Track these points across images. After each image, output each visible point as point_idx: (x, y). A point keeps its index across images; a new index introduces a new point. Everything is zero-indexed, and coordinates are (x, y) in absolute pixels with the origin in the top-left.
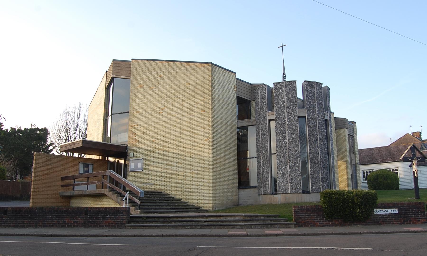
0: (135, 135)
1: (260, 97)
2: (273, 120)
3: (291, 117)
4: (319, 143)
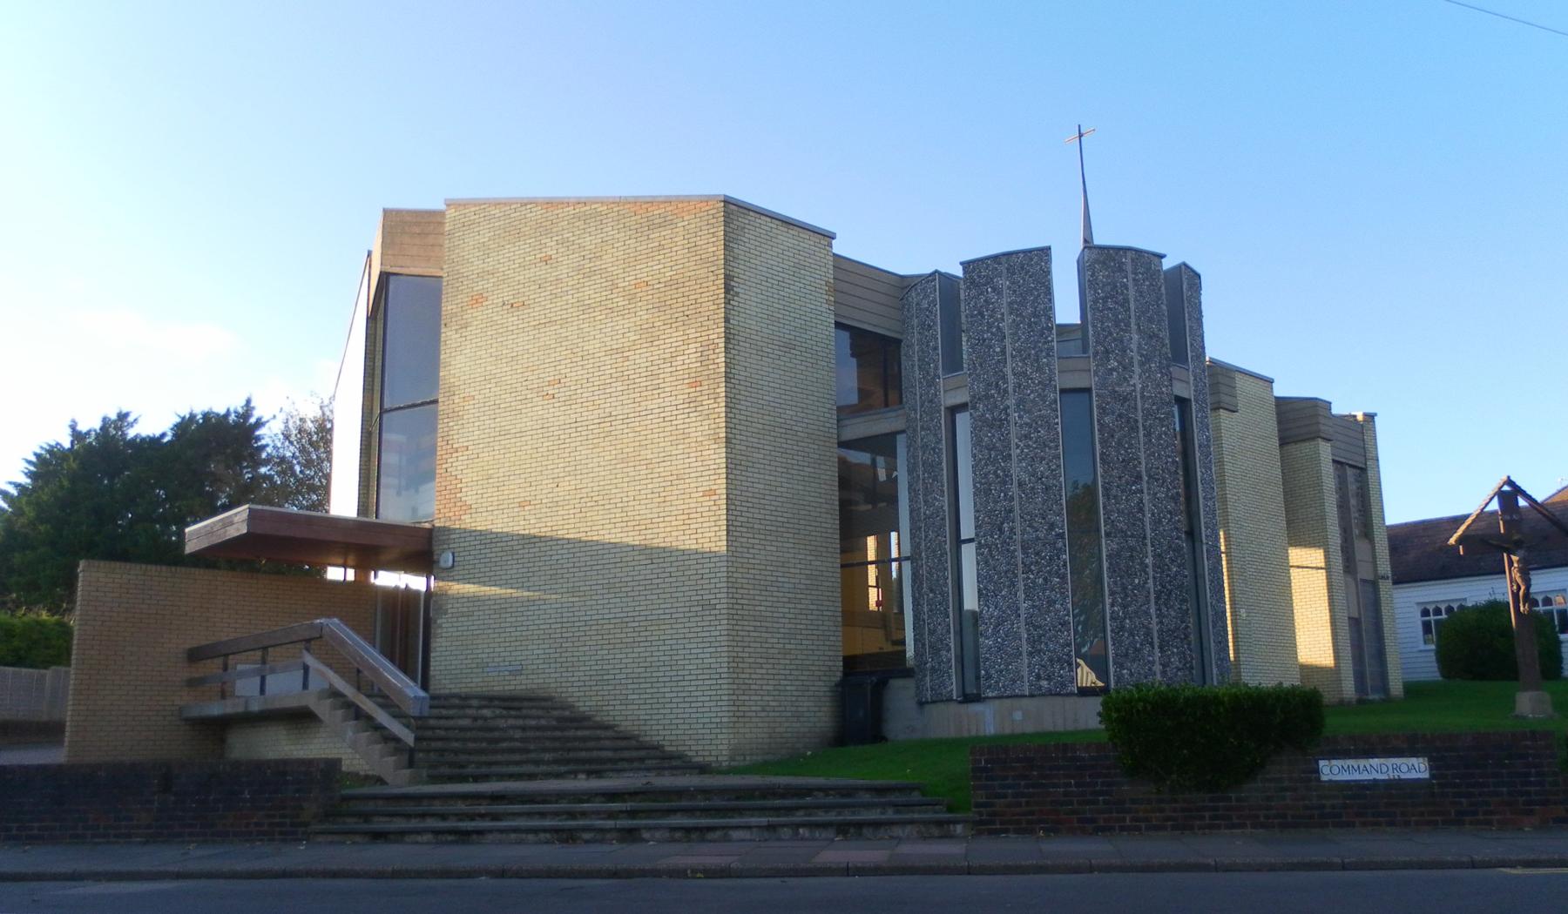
0: (459, 486)
1: (916, 320)
2: (962, 407)
3: (1032, 392)
4: (1145, 491)
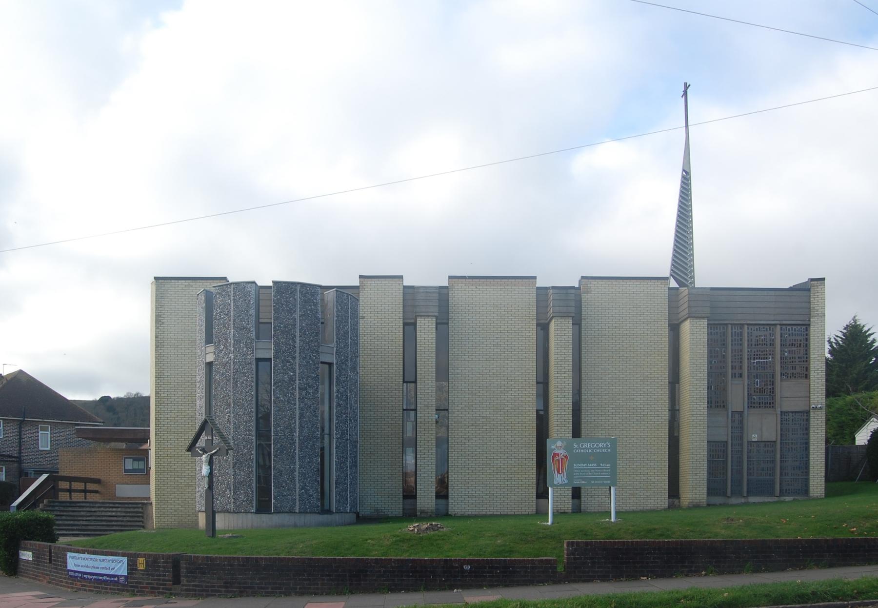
4: (232, 412)
